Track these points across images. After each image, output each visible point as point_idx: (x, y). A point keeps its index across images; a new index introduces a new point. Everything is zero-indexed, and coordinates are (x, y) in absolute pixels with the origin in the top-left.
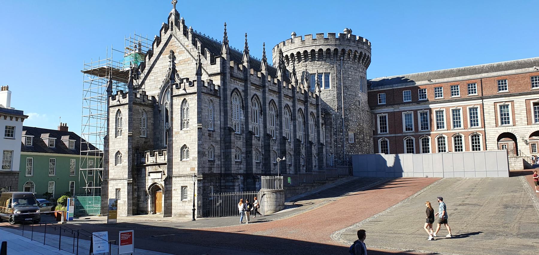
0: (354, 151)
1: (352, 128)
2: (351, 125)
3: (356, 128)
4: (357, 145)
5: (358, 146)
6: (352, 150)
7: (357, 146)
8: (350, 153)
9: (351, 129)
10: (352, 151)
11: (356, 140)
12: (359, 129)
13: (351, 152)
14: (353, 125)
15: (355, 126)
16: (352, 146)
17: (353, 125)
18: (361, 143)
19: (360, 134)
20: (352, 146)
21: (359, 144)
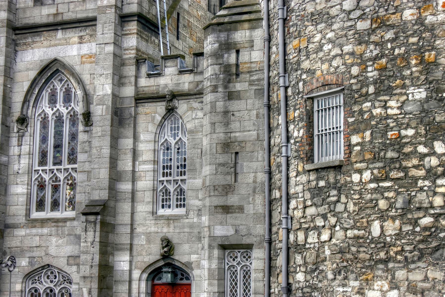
0: (333, 220)
1: (325, 67)
2: (320, 48)
3: (352, 54)
4: (360, 172)
5: (367, 175)
6: (322, 210)
7: (356, 178)
8: (312, 238)
9: (318, 73)
10: (324, 217)
11: (355, 139)
12: (375, 59)
13: (316, 228)
14: (330, 41)
15: (341, 46)
16: (322, 183)
17: (330, 41)
18: (390, 154)
19: (377, 93)
20: (322, 183)
21: (375, 159)
